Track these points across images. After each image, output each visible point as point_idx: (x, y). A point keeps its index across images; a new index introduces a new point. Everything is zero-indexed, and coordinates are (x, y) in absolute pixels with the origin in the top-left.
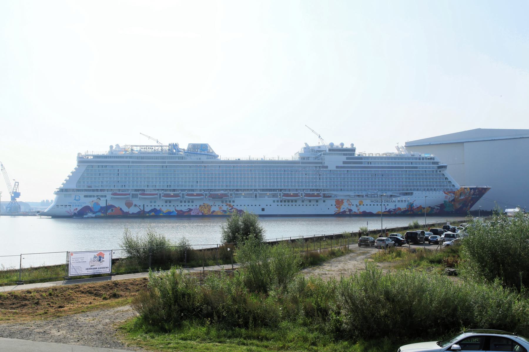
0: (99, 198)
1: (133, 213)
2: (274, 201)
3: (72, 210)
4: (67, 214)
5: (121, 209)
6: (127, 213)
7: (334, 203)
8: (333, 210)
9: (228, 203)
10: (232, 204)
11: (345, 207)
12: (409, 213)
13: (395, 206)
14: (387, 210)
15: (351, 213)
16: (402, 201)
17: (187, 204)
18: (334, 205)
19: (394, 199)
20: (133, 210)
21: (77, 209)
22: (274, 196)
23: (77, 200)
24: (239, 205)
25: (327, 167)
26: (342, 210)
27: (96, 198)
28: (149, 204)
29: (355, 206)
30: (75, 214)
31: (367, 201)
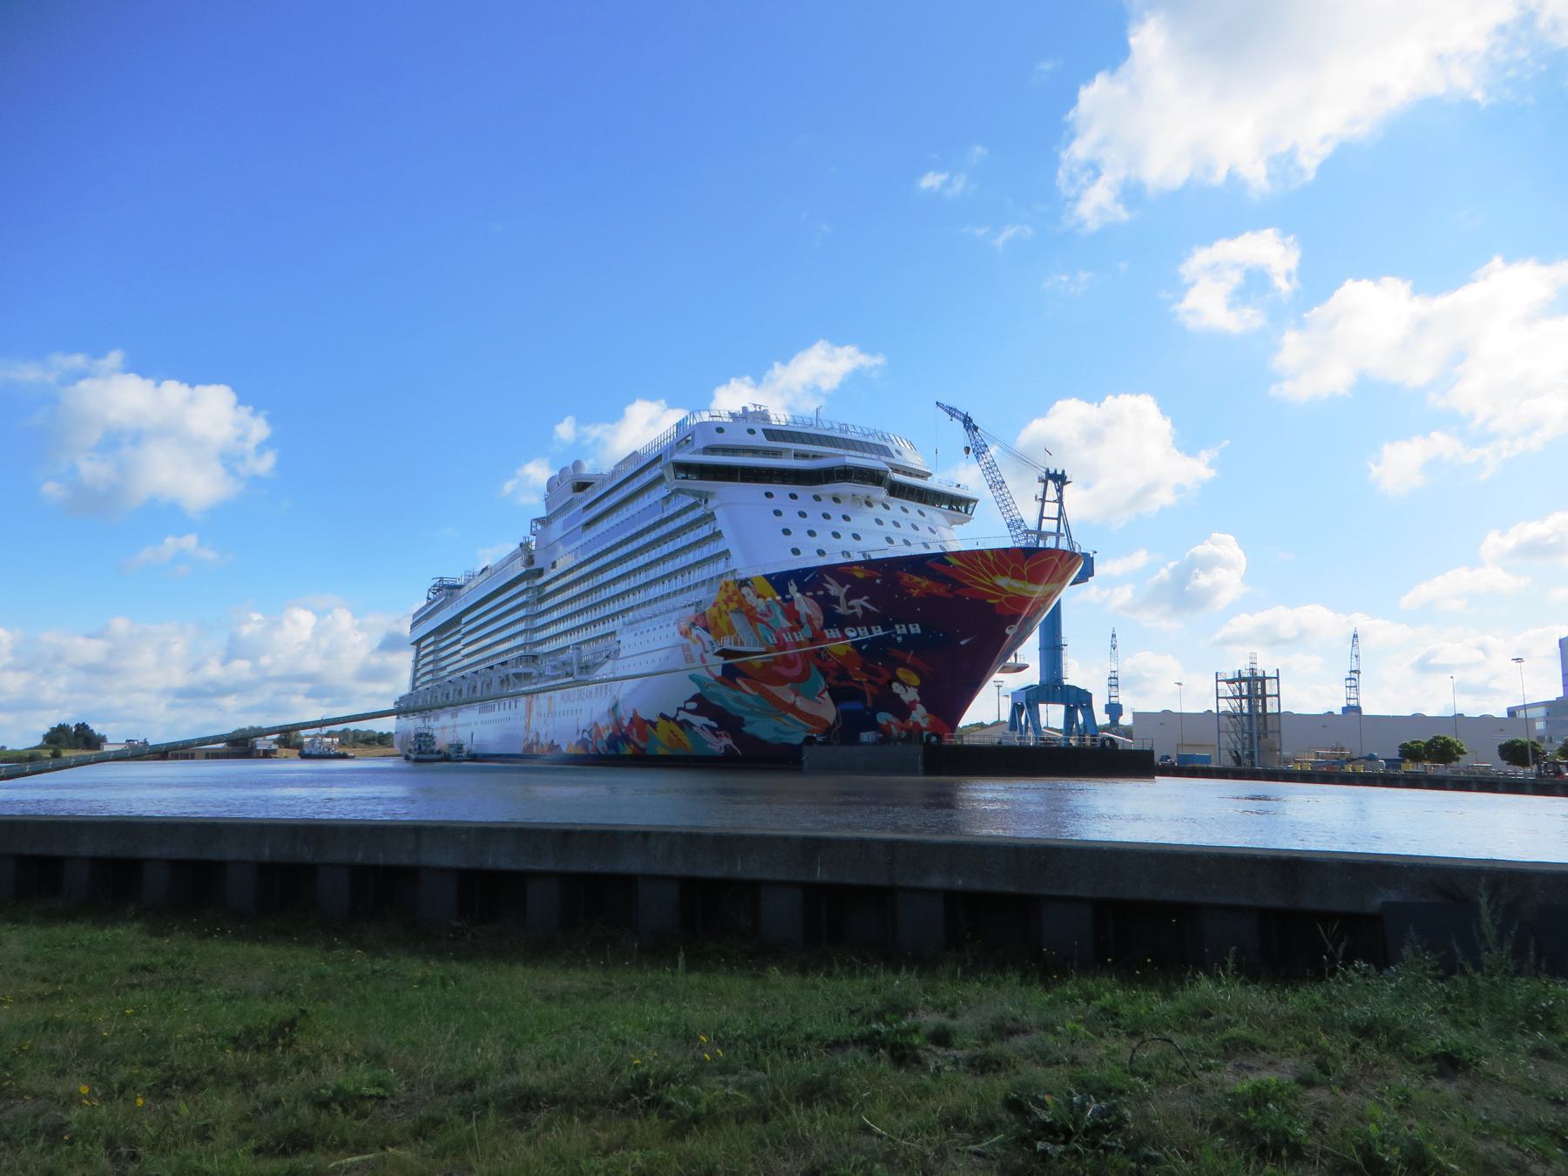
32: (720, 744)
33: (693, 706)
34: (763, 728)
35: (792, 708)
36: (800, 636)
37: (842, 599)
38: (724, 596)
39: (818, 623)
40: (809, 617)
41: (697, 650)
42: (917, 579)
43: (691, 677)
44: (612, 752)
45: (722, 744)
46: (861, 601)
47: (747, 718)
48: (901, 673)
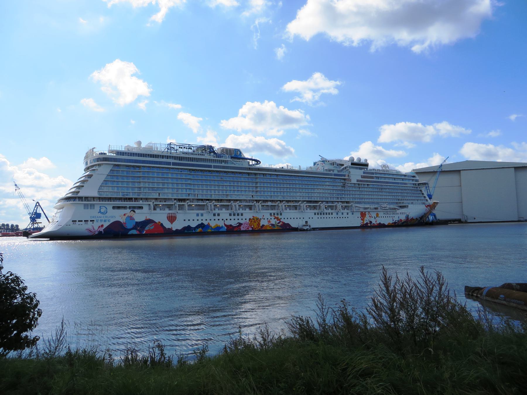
0: (133, 209)
1: (177, 230)
2: (315, 214)
3: (96, 227)
4: (87, 233)
5: (162, 224)
6: (170, 230)
8: (358, 222)
11: (367, 219)
17: (236, 217)
19: (398, 211)
20: (177, 226)
21: (102, 226)
22: (315, 208)
23: (103, 213)
24: (286, 218)
26: (365, 222)
27: (128, 211)
28: (196, 218)
30: (100, 232)
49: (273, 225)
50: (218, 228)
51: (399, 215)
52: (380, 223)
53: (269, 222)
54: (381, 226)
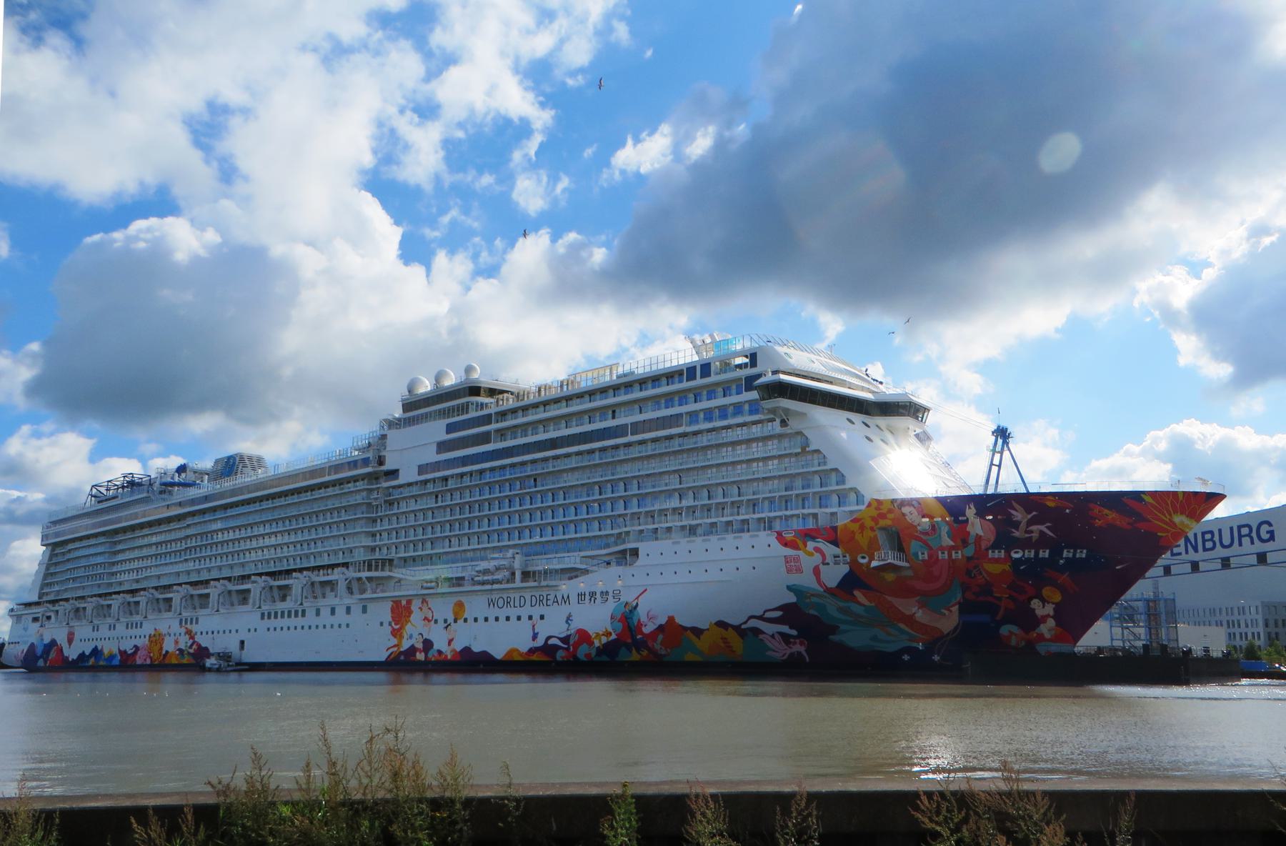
7: (388, 617)
9: (189, 626)
10: (194, 628)
11: (415, 631)
12: (635, 656)
13: (568, 619)
14: (540, 642)
15: (430, 655)
16: (593, 594)
18: (386, 624)
19: (565, 587)
20: (72, 653)
25: (393, 473)
26: (406, 645)
29: (441, 624)
31: (476, 606)
32: (779, 652)
33: (779, 614)
34: (855, 638)
35: (910, 620)
36: (956, 555)
37: (1023, 526)
38: (875, 513)
39: (983, 546)
40: (978, 538)
41: (808, 560)
42: (1106, 511)
43: (789, 588)
44: (605, 658)
45: (788, 652)
46: (1043, 528)
47: (843, 627)
48: (1046, 592)
49: (180, 650)
50: (112, 657)
51: (574, 608)
52: (467, 650)
53: (176, 642)
54: (473, 664)
